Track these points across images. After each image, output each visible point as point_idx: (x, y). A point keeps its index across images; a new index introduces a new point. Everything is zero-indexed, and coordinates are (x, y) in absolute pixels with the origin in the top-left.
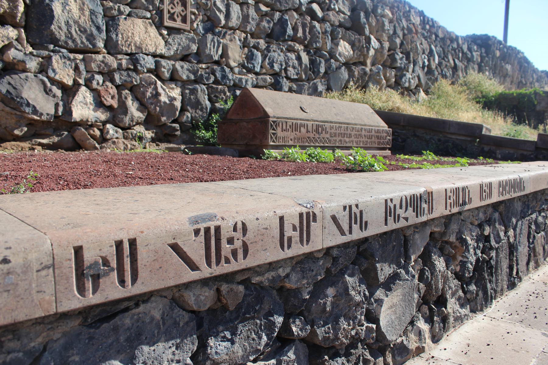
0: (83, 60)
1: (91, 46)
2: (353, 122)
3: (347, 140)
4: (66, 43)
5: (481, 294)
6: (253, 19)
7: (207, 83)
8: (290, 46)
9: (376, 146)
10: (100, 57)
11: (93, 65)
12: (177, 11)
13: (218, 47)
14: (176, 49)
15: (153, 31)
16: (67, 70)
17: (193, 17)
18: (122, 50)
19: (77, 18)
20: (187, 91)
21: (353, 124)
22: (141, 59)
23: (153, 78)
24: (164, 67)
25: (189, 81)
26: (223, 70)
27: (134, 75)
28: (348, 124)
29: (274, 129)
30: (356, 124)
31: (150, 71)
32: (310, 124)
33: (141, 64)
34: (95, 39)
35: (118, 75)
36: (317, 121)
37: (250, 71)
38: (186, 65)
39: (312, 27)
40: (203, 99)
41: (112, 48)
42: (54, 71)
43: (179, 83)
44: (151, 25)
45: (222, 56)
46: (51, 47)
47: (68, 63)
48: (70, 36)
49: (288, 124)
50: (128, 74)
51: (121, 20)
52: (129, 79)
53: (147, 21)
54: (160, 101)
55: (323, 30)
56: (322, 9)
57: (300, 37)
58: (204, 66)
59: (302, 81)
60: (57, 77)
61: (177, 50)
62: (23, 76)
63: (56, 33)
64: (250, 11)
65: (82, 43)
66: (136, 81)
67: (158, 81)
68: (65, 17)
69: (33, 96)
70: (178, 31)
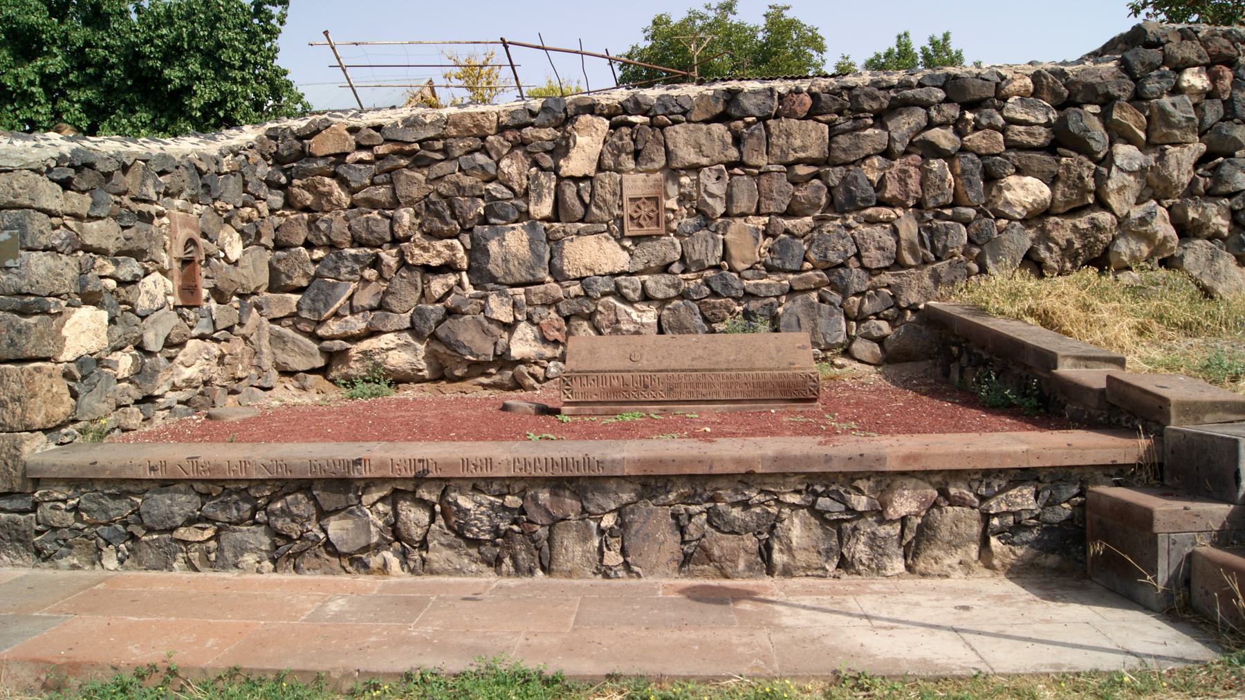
2: (724, 367)
3: (704, 391)
5: (507, 560)
6: (780, 192)
8: (870, 216)
10: (542, 288)
12: (643, 213)
13: (715, 246)
15: (611, 247)
17: (671, 216)
20: (665, 312)
25: (667, 300)
26: (723, 277)
27: (586, 302)
30: (727, 370)
32: (627, 376)
37: (770, 269)
38: (665, 279)
39: (925, 173)
41: (558, 275)
44: (608, 239)
45: (723, 258)
46: (490, 286)
48: (508, 273)
51: (567, 243)
52: (577, 308)
53: (600, 236)
54: (620, 330)
55: (959, 171)
56: (960, 133)
57: (894, 197)
59: (911, 267)
60: (494, 316)
64: (774, 182)
67: (618, 304)
69: (469, 338)
70: (649, 237)
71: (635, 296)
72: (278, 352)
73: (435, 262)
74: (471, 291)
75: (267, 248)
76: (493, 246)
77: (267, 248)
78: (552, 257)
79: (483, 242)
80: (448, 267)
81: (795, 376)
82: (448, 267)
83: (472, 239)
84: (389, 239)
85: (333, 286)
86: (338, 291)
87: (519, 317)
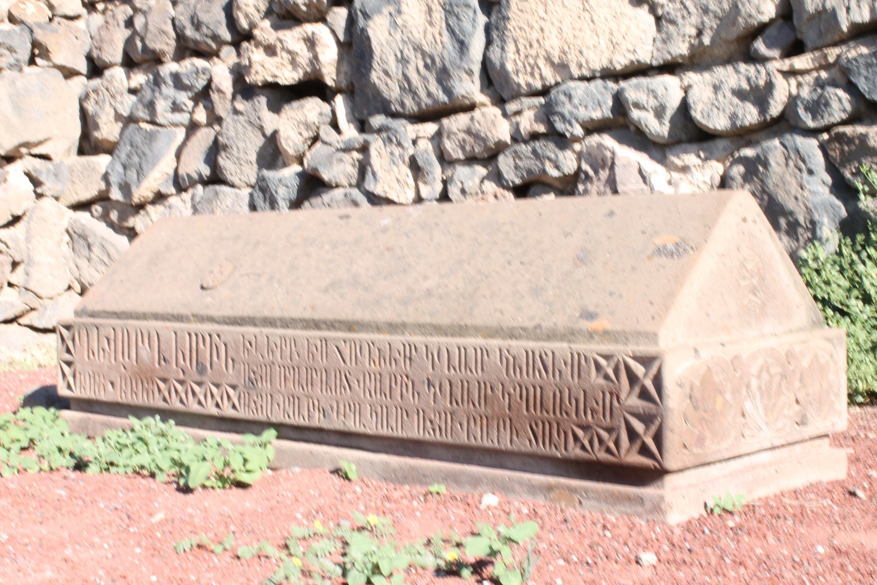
0: (439, 134)
1: (443, 97)
2: (384, 315)
4: (402, 104)
7: (811, 124)
9: (524, 444)
11: (449, 145)
14: (693, 32)
16: (395, 168)
18: (519, 85)
19: (418, 36)
21: (378, 328)
22: (562, 98)
23: (606, 148)
24: (637, 105)
27: (549, 149)
28: (350, 326)
29: (68, 351)
30: (393, 327)
31: (593, 128)
33: (563, 117)
34: (449, 76)
35: (511, 161)
36: (211, 319)
40: (794, 188)
42: (374, 174)
43: (721, 144)
46: (378, 120)
47: (397, 151)
49: (103, 332)
50: (534, 152)
58: (801, 62)
60: (378, 190)
61: (700, 33)
62: (326, 197)
63: (382, 87)
65: (429, 94)
66: (557, 167)
68: (394, 45)
71: (659, 128)
72: (83, 263)
73: (288, 77)
74: (350, 131)
75: (69, 73)
76: (378, 31)
77: (69, 73)
78: (489, 42)
79: (361, 22)
80: (312, 87)
81: (578, 364)
82: (312, 87)
83: (351, 21)
84: (227, 36)
85: (151, 137)
86: (159, 145)
87: (425, 191)
